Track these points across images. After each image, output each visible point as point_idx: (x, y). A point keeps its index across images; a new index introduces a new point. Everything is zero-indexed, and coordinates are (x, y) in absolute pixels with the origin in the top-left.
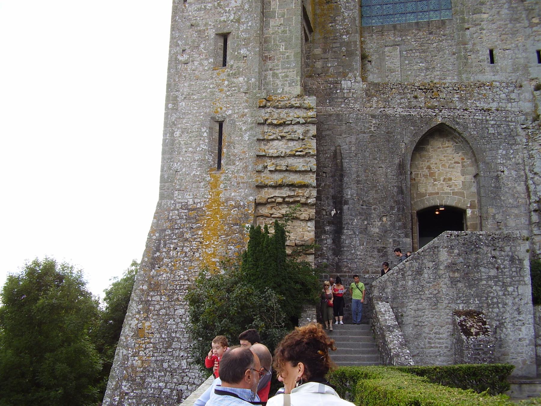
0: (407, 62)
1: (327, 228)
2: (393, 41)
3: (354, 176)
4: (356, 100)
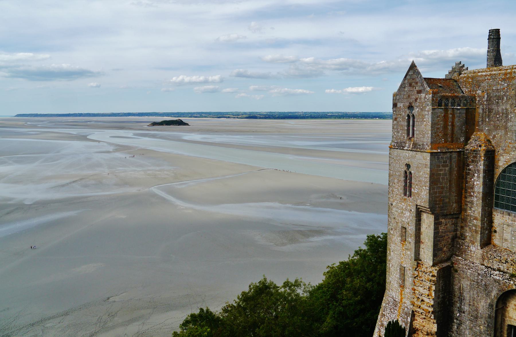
0: (513, 238)
1: (455, 321)
2: (508, 222)
3: (468, 301)
4: (477, 258)
